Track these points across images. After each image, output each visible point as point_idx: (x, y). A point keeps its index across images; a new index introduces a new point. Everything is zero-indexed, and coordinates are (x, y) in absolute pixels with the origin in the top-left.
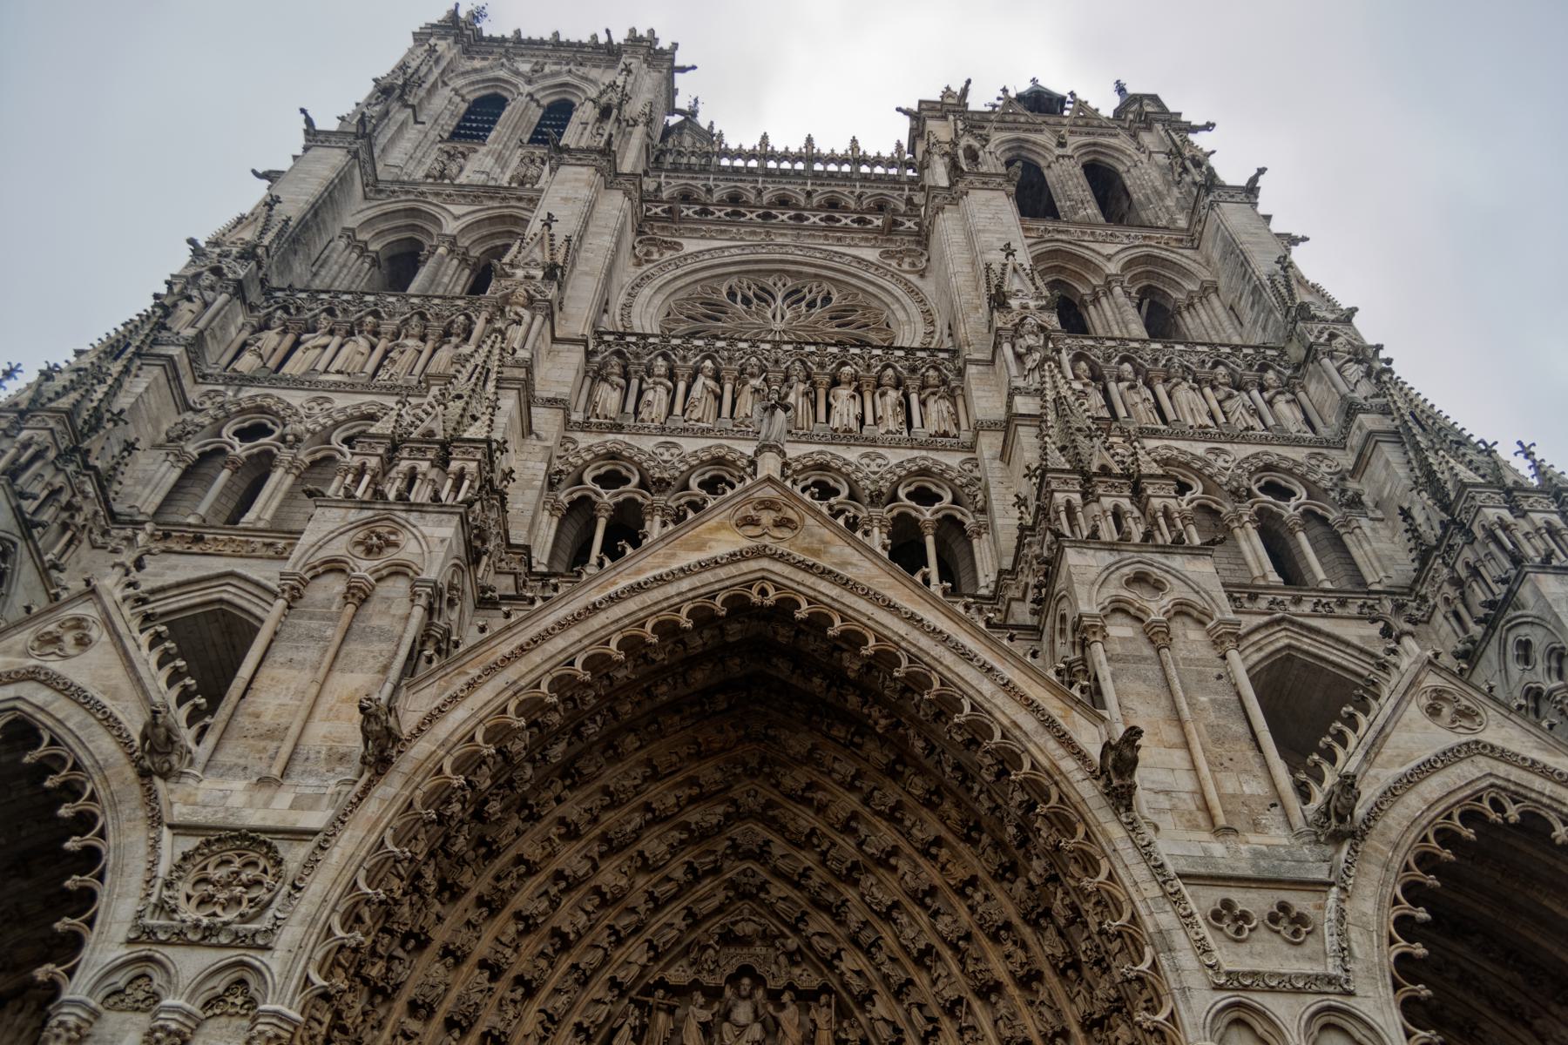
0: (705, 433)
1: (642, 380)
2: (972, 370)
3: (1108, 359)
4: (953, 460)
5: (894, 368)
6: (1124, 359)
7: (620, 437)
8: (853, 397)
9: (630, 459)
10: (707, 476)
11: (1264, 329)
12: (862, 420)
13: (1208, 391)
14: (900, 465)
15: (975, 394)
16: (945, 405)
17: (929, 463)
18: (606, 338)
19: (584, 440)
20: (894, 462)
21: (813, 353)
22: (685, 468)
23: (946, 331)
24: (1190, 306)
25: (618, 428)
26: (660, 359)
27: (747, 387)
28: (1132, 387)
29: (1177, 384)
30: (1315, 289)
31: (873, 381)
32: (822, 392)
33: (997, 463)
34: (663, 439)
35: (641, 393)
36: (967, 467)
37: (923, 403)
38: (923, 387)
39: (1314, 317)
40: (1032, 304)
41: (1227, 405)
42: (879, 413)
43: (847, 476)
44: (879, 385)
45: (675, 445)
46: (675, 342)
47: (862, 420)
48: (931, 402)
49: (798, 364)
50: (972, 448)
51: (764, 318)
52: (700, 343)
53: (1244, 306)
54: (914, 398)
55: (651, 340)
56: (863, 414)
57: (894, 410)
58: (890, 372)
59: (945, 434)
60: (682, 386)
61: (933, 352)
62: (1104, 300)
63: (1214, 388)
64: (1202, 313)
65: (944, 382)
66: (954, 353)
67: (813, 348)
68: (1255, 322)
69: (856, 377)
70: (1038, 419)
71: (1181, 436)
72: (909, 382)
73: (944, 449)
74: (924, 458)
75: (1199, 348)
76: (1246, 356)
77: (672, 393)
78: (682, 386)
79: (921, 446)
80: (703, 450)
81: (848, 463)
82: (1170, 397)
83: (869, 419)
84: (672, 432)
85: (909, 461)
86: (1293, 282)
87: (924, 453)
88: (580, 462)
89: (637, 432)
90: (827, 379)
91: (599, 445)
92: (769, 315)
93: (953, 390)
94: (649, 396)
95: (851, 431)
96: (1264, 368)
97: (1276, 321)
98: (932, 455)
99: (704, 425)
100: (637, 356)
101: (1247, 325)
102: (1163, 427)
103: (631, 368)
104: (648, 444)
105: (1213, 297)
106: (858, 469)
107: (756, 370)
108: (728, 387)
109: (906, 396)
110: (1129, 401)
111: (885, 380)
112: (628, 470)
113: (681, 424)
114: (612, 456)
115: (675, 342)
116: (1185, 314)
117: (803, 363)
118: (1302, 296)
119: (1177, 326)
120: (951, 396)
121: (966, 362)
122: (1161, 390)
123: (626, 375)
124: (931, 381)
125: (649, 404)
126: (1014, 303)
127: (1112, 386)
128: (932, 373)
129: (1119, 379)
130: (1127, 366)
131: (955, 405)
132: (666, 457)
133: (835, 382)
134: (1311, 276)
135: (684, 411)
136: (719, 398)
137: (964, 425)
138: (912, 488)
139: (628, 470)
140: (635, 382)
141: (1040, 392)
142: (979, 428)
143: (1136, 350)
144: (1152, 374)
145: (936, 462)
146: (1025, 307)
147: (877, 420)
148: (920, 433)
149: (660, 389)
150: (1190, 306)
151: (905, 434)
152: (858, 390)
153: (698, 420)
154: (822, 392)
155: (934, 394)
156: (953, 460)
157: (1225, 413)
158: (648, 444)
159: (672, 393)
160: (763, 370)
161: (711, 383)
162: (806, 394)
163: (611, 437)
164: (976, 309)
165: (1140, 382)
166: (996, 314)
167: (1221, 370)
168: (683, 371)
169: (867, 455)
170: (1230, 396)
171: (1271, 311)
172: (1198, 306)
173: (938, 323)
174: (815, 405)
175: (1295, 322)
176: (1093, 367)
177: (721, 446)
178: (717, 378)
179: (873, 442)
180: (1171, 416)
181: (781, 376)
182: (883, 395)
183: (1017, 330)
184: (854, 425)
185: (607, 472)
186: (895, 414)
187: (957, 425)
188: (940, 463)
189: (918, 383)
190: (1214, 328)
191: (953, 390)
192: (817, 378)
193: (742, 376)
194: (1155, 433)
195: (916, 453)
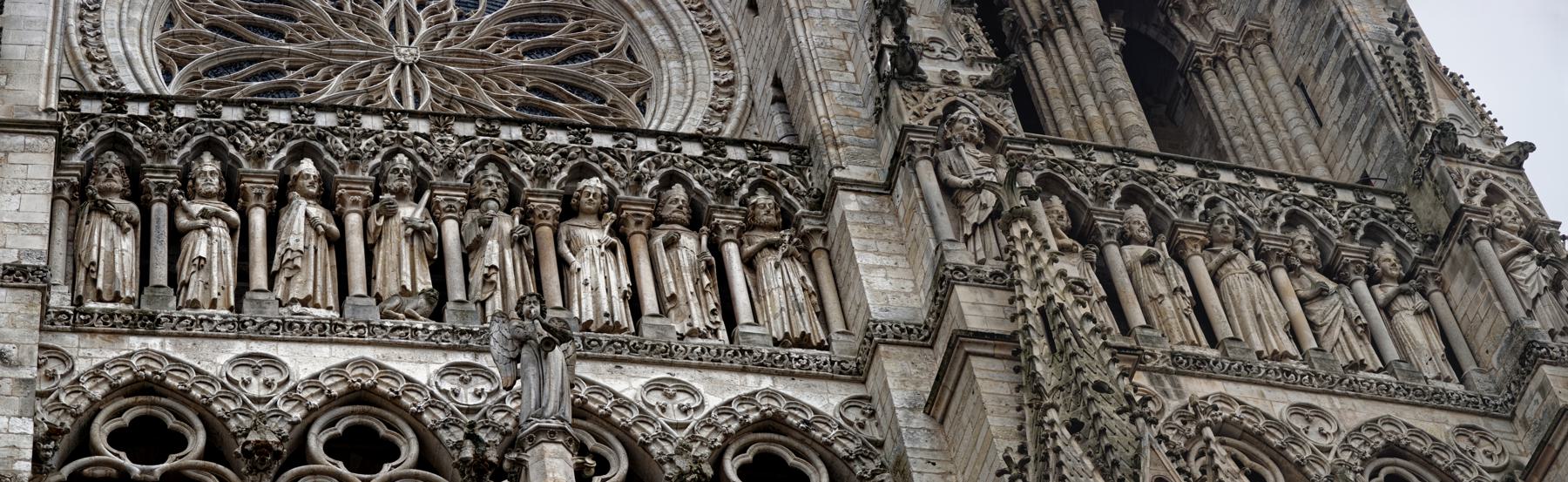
0: (324, 333)
1: (173, 205)
2: (849, 203)
3: (1103, 193)
4: (825, 399)
5: (687, 184)
6: (1131, 196)
7: (154, 343)
8: (612, 248)
9: (184, 395)
10: (340, 428)
11: (1367, 146)
12: (634, 301)
13: (1281, 275)
14: (725, 408)
15: (862, 259)
16: (796, 273)
17: (781, 406)
18: (87, 107)
19: (89, 353)
20: (713, 401)
21: (517, 144)
22: (297, 415)
23: (764, 89)
24: (1219, 61)
25: (148, 324)
26: (207, 158)
27: (395, 222)
28: (1149, 260)
29: (1230, 259)
30: (1456, 86)
31: (647, 212)
32: (546, 232)
33: (920, 420)
34: (240, 348)
35: (176, 238)
36: (854, 415)
37: (750, 263)
38: (750, 224)
39: (1464, 150)
40: (964, 73)
41: (1317, 308)
42: (670, 287)
43: (624, 434)
44: (658, 221)
45: (272, 362)
46: (231, 114)
47: (634, 301)
48: (768, 262)
49: (491, 169)
50: (858, 374)
51: (373, 31)
52: (280, 117)
53: (1327, 86)
54: (732, 252)
55: (180, 111)
56: (634, 286)
57: (697, 282)
58: (678, 191)
59: (804, 341)
60: (258, 219)
61: (758, 148)
62: (1061, 36)
63: (1292, 271)
64: (1242, 79)
65: (787, 219)
66: (802, 153)
67: (516, 133)
68: (1348, 128)
69: (610, 202)
70: (1010, 347)
71: (1244, 374)
72: (719, 217)
73: (803, 374)
74: (770, 394)
75: (1262, 182)
76: (1343, 206)
77: (241, 233)
78: (258, 219)
79: (762, 367)
80: (329, 372)
81: (622, 403)
82: (1216, 284)
83: (650, 303)
84: (262, 331)
85: (742, 400)
86: (1422, 69)
87: (767, 383)
88: (84, 403)
89: (188, 330)
90: (555, 206)
91: (116, 363)
92: (384, 25)
93: (806, 237)
94: (200, 246)
95: (617, 328)
96: (1375, 234)
97: (1391, 137)
98: (784, 387)
99: (322, 313)
100: (161, 152)
101: (1329, 119)
102: (1213, 353)
103: (151, 179)
104: (217, 358)
105: (1263, 51)
106: (644, 418)
107: (407, 183)
108: (354, 220)
109: (715, 247)
110: (1145, 288)
111: (669, 211)
112: (179, 416)
113: (273, 312)
114: (145, 387)
115: (231, 114)
116: (1210, 76)
117: (503, 167)
118: (1444, 108)
119: (1192, 99)
120: (803, 252)
121: (837, 184)
122: (1200, 266)
123: (137, 193)
124: (763, 217)
125: (202, 264)
126: (930, 68)
127: (1113, 251)
128: (762, 198)
129: (1125, 239)
130: (1136, 212)
131: (812, 269)
132: (256, 389)
133: (570, 210)
134: (1450, 60)
135: (272, 278)
136: (338, 245)
137: (837, 324)
138: (748, 457)
139: (179, 416)
140: (160, 210)
141: (1004, 280)
142: (876, 338)
143: (1152, 178)
144: (1183, 233)
145: (793, 403)
146: (950, 80)
147: (667, 303)
148: (757, 335)
149: (218, 228)
150: (1219, 61)
151: (723, 334)
152: (617, 230)
153: (304, 303)
154: (546, 232)
155: (772, 246)
156: (825, 399)
157: (1312, 325)
158: (217, 358)
159: (241, 233)
160: (421, 185)
161: (317, 212)
162: (517, 241)
163: (135, 343)
164: (842, 60)
165: (1162, 250)
166: (896, 92)
167: (1303, 234)
168: (258, 185)
169: (656, 386)
170: (1322, 294)
171: (1381, 117)
172: (1234, 63)
173: (742, 62)
174: (536, 264)
175: (1429, 152)
176: (1074, 206)
177: (364, 363)
178: (327, 197)
179: (664, 355)
180: (1223, 330)
181: (460, 197)
182: (670, 244)
183: (943, 139)
184: (621, 313)
185: (134, 421)
186: (701, 292)
187: (823, 316)
188: (803, 407)
189: (738, 220)
190: (1266, 117)
191: (806, 237)
192: (535, 203)
193: (378, 199)
194: (1199, 367)
195: (751, 383)
